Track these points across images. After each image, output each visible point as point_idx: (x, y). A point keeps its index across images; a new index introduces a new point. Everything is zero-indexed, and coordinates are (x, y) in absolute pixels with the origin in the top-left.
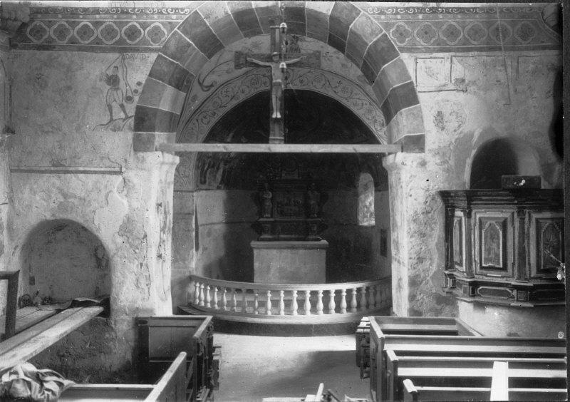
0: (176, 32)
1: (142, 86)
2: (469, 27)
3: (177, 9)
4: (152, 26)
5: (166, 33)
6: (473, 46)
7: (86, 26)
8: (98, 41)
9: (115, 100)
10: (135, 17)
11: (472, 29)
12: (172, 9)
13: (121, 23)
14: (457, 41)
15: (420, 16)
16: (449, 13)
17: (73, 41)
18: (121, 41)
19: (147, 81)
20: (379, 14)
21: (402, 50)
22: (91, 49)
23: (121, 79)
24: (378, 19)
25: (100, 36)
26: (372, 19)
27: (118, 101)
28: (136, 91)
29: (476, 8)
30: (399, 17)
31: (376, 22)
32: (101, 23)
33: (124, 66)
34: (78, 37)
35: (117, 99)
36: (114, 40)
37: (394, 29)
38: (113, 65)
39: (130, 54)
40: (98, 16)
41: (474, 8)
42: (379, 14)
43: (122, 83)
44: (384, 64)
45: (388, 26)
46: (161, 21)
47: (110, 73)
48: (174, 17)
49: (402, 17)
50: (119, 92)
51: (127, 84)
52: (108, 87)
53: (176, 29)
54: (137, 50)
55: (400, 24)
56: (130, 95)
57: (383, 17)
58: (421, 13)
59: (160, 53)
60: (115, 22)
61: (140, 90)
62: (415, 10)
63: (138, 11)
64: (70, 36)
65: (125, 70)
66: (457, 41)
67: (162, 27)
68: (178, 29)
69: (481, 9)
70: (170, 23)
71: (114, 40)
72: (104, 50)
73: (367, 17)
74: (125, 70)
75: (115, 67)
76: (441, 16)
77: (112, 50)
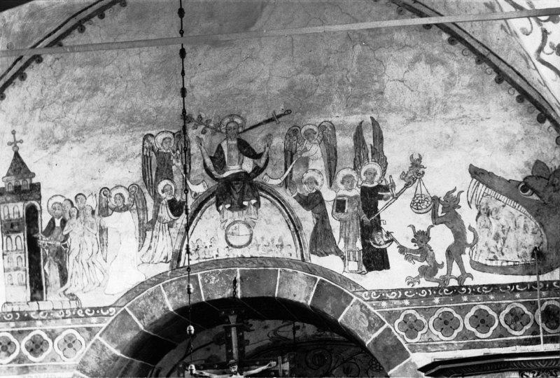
0: (97, 340)
2: (507, 310)
3: (99, 308)
6: (514, 338)
10: (39, 323)
11: (511, 313)
12: (92, 309)
13: (20, 332)
14: (491, 332)
15: (437, 300)
16: (476, 293)
18: (20, 359)
20: (378, 300)
21: (414, 348)
24: (376, 307)
26: (369, 307)
29: (515, 284)
30: (406, 302)
31: (375, 311)
37: (401, 319)
41: (511, 285)
42: (378, 300)
44: (389, 369)
45: (391, 316)
48: (94, 320)
49: (411, 303)
53: (97, 336)
55: (409, 312)
57: (384, 304)
58: (437, 295)
60: (12, 333)
62: (428, 293)
63: (45, 314)
66: (491, 332)
69: (523, 285)
70: (89, 329)
73: (362, 305)
76: (465, 298)
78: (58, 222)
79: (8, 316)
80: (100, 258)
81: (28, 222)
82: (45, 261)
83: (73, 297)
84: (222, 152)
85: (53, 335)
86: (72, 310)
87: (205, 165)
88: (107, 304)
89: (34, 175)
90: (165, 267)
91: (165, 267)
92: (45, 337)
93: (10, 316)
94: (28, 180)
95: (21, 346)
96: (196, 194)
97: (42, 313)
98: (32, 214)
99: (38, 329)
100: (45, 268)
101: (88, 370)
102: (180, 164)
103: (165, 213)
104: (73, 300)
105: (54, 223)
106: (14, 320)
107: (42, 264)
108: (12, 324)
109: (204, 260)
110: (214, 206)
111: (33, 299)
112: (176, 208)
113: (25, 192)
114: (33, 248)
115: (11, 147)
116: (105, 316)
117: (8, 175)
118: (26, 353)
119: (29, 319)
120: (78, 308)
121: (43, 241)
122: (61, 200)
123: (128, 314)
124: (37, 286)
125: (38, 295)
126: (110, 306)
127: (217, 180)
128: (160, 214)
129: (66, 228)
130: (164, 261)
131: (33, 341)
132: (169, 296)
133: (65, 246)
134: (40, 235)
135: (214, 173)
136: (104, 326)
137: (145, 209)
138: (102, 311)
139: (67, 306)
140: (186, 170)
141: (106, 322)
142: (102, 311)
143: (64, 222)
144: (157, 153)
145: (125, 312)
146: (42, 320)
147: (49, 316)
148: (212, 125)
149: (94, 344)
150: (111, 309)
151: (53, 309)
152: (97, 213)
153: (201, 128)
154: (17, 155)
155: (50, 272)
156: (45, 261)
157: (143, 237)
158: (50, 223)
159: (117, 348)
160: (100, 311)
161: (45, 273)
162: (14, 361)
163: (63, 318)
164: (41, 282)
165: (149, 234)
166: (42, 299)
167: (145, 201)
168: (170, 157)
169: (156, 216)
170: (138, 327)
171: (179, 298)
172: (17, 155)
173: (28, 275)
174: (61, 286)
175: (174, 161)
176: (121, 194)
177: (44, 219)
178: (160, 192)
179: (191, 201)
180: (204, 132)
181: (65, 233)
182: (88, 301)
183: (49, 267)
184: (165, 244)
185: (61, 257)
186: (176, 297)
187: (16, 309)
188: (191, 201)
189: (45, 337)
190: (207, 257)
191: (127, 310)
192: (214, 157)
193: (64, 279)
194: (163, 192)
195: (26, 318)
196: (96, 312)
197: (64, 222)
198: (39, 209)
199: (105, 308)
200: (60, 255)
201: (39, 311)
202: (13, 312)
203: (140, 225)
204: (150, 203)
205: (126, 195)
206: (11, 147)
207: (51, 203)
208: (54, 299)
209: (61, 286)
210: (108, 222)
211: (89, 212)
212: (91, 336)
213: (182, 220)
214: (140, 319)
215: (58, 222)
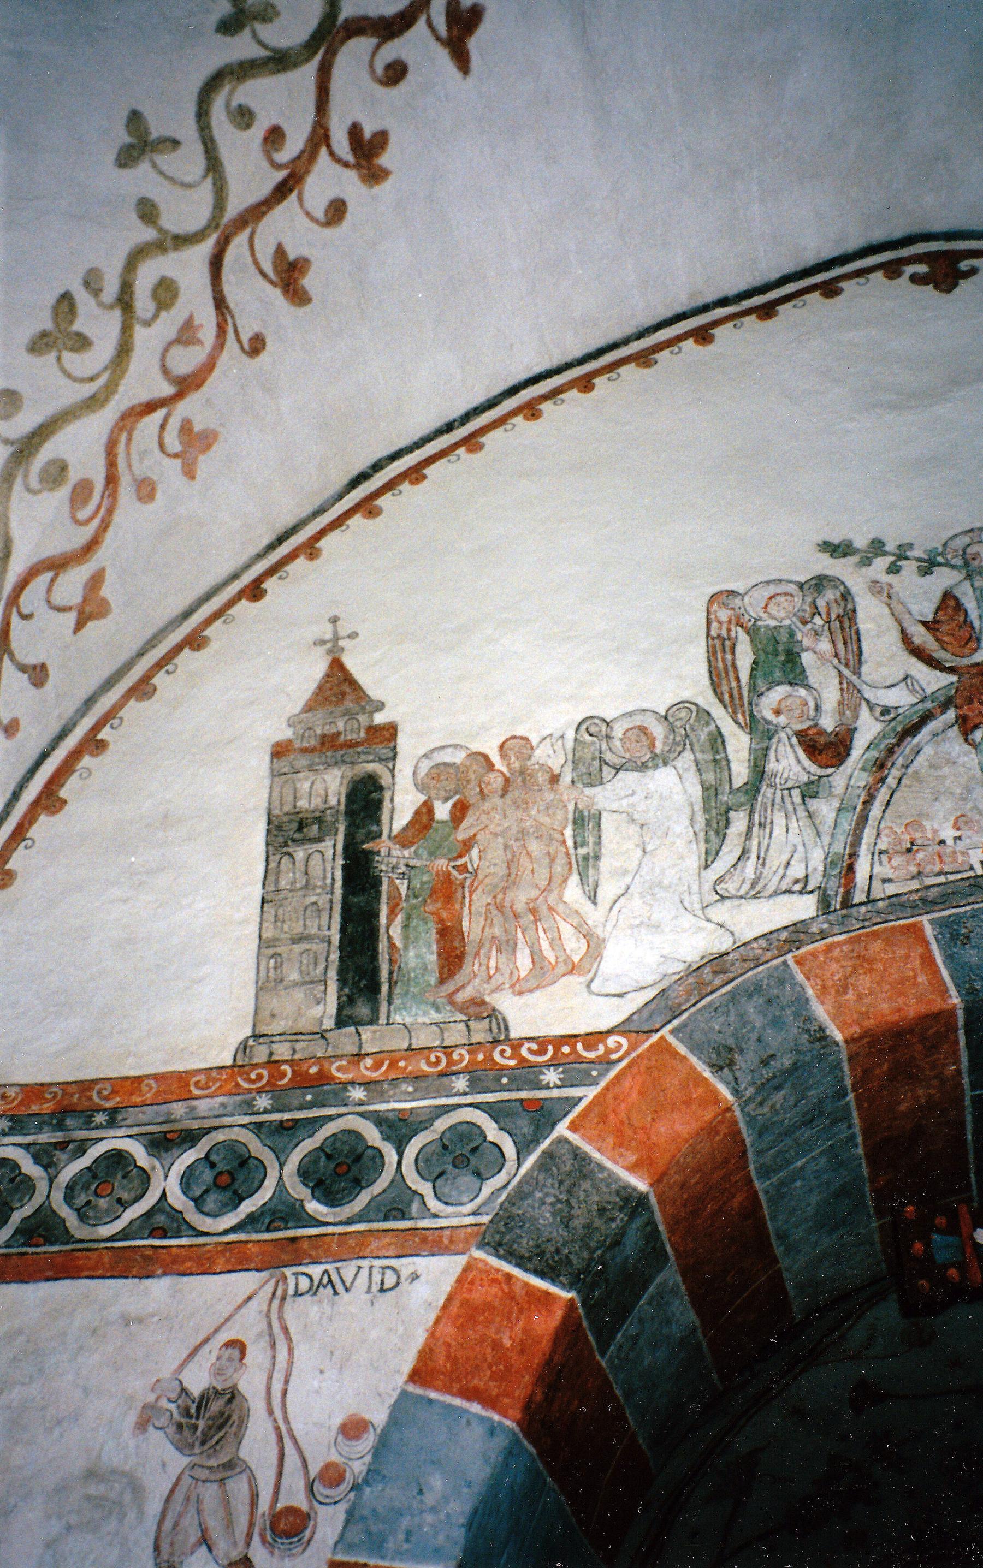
0: (562, 1140)
1: (369, 1441)
4: (442, 1124)
5: (509, 1149)
7: (118, 1159)
8: (163, 1221)
9: (205, 1540)
10: (357, 1094)
12: (542, 1043)
17: (43, 1227)
18: (283, 1213)
19: (402, 1409)
22: (127, 1263)
23: (257, 1405)
25: (177, 1199)
27: (222, 1546)
28: (332, 1475)
32: (190, 1138)
33: (278, 1334)
34: (66, 1212)
35: (214, 1524)
36: (248, 1207)
38: (224, 1337)
39: (316, 1271)
40: (178, 1109)
43: (256, 1444)
46: (489, 1097)
47: (198, 1380)
48: (551, 1076)
50: (239, 1487)
51: (283, 1436)
52: (178, 1462)
53: (562, 1129)
54: (350, 1247)
56: (301, 1502)
59: (478, 1254)
60: (258, 1128)
61: (358, 1468)
63: (377, 1066)
64: (27, 1210)
65: (282, 1355)
67: (492, 1131)
68: (573, 1127)
71: (248, 1207)
72: (200, 1263)
74: (282, 1355)
75: (230, 1344)
77: (236, 1259)
78: (442, 811)
79: (253, 1076)
80: (573, 892)
81: (349, 813)
82: (392, 913)
83: (479, 1009)
84: (959, 607)
85: (399, 1129)
86: (474, 1048)
87: (906, 639)
88: (604, 1026)
89: (380, 706)
90: (804, 908)
91: (804, 908)
92: (372, 1135)
93: (260, 1077)
94: (361, 718)
95: (282, 1176)
96: (886, 711)
97: (369, 1062)
98: (365, 800)
99: (350, 1120)
100: (392, 929)
101: (525, 1245)
102: (824, 645)
103: (789, 763)
104: (480, 1018)
105: (430, 811)
106: (271, 1088)
107: (383, 920)
108: (263, 1102)
109: (942, 879)
110: (954, 732)
111: (341, 1022)
112: (827, 748)
113: (351, 745)
114: (360, 875)
115: (321, 650)
116: (592, 1062)
117: (309, 708)
118: (298, 1191)
119: (324, 1078)
120: (496, 1042)
121: (390, 856)
122: (458, 757)
123: (675, 1054)
124: (361, 974)
125: (363, 1010)
126: (610, 1032)
127: (951, 670)
128: (772, 766)
129: (465, 824)
130: (797, 887)
131: (326, 1152)
132: (823, 991)
133: (463, 869)
134: (383, 845)
135: (940, 654)
136: (590, 1093)
137: (720, 762)
138: (579, 1047)
139: (456, 1035)
140: (851, 652)
141: (594, 1083)
142: (579, 1047)
143: (460, 811)
144: (752, 632)
145: (663, 1047)
146: (367, 1084)
147: (397, 1069)
148: (917, 553)
149: (549, 1155)
150: (611, 1041)
151: (409, 1049)
152: (567, 778)
153: (881, 563)
154: (337, 665)
155: (407, 944)
156: (392, 913)
157: (716, 827)
158: (417, 813)
159: (631, 1168)
160: (573, 1048)
161: (392, 946)
162: (251, 1221)
163: (443, 1074)
164: (376, 971)
165: (739, 822)
166: (373, 1021)
167: (717, 740)
168: (792, 634)
169: (759, 772)
170: (714, 1096)
171: (860, 997)
172: (337, 665)
173: (335, 956)
174: (442, 981)
175: (806, 642)
176: (643, 730)
177: (402, 804)
178: (769, 715)
179: (868, 729)
180: (894, 569)
181: (461, 835)
182: (534, 1014)
183: (406, 927)
184: (796, 845)
185: (449, 898)
186: (850, 995)
187: (282, 1051)
188: (868, 729)
189: (372, 1135)
190: (946, 869)
191: (671, 1039)
192: (935, 621)
193: (452, 958)
194: (778, 712)
195: (318, 1084)
196: (557, 1049)
197: (460, 811)
198: (385, 781)
199: (592, 1039)
200: (446, 890)
201: (359, 1056)
202: (272, 1063)
203: (706, 800)
204: (739, 745)
205: (658, 731)
206: (321, 650)
207: (425, 766)
208: (414, 1020)
209: (442, 981)
210: (610, 796)
211: (542, 778)
212: (538, 1127)
213: (851, 774)
214: (717, 1068)
215: (442, 811)
